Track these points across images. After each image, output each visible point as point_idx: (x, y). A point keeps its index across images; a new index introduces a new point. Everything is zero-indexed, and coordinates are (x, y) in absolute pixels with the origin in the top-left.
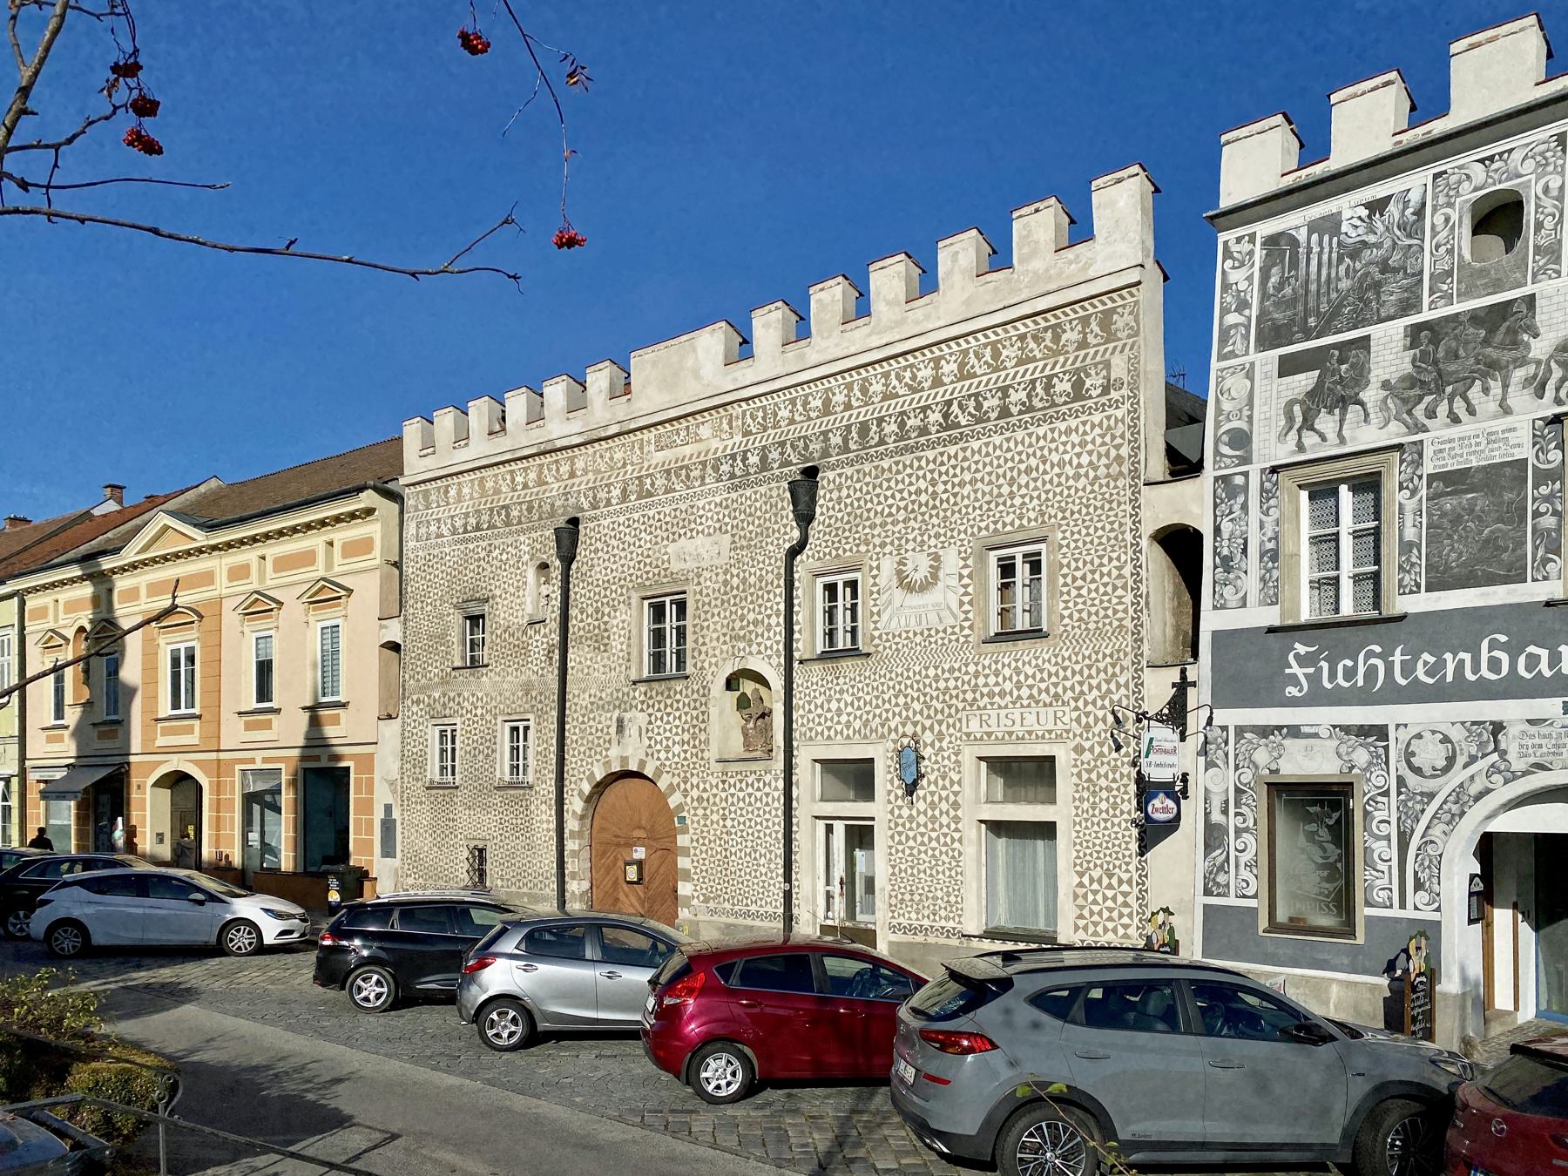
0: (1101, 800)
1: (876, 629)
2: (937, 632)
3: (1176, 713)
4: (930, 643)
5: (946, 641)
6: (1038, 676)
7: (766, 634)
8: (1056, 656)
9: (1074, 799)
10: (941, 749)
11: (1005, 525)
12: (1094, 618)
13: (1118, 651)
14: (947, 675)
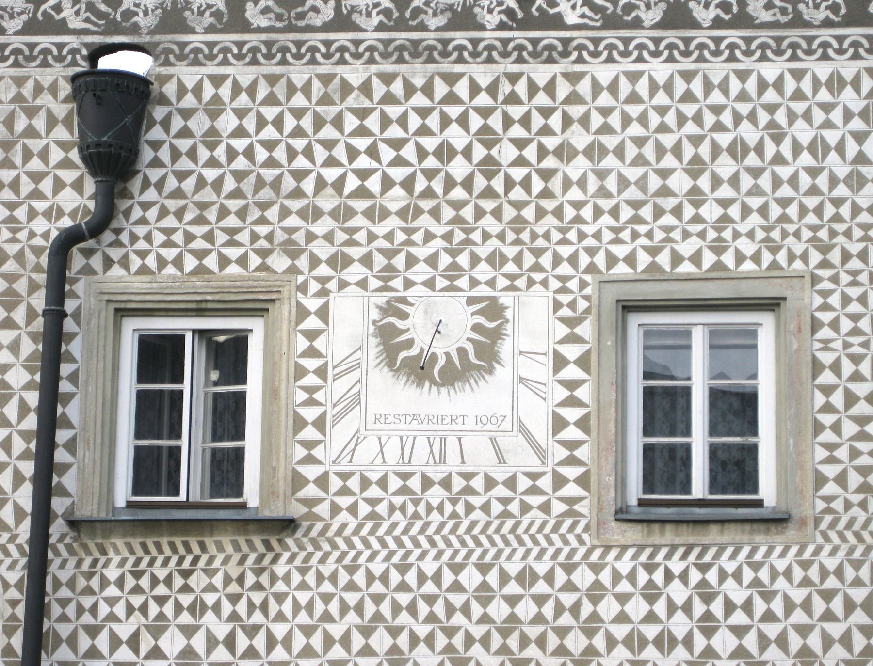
1: (310, 460)
2: (490, 483)
4: (469, 508)
5: (514, 508)
6: (759, 606)
8: (805, 565)
11: (676, 259)
14: (513, 588)
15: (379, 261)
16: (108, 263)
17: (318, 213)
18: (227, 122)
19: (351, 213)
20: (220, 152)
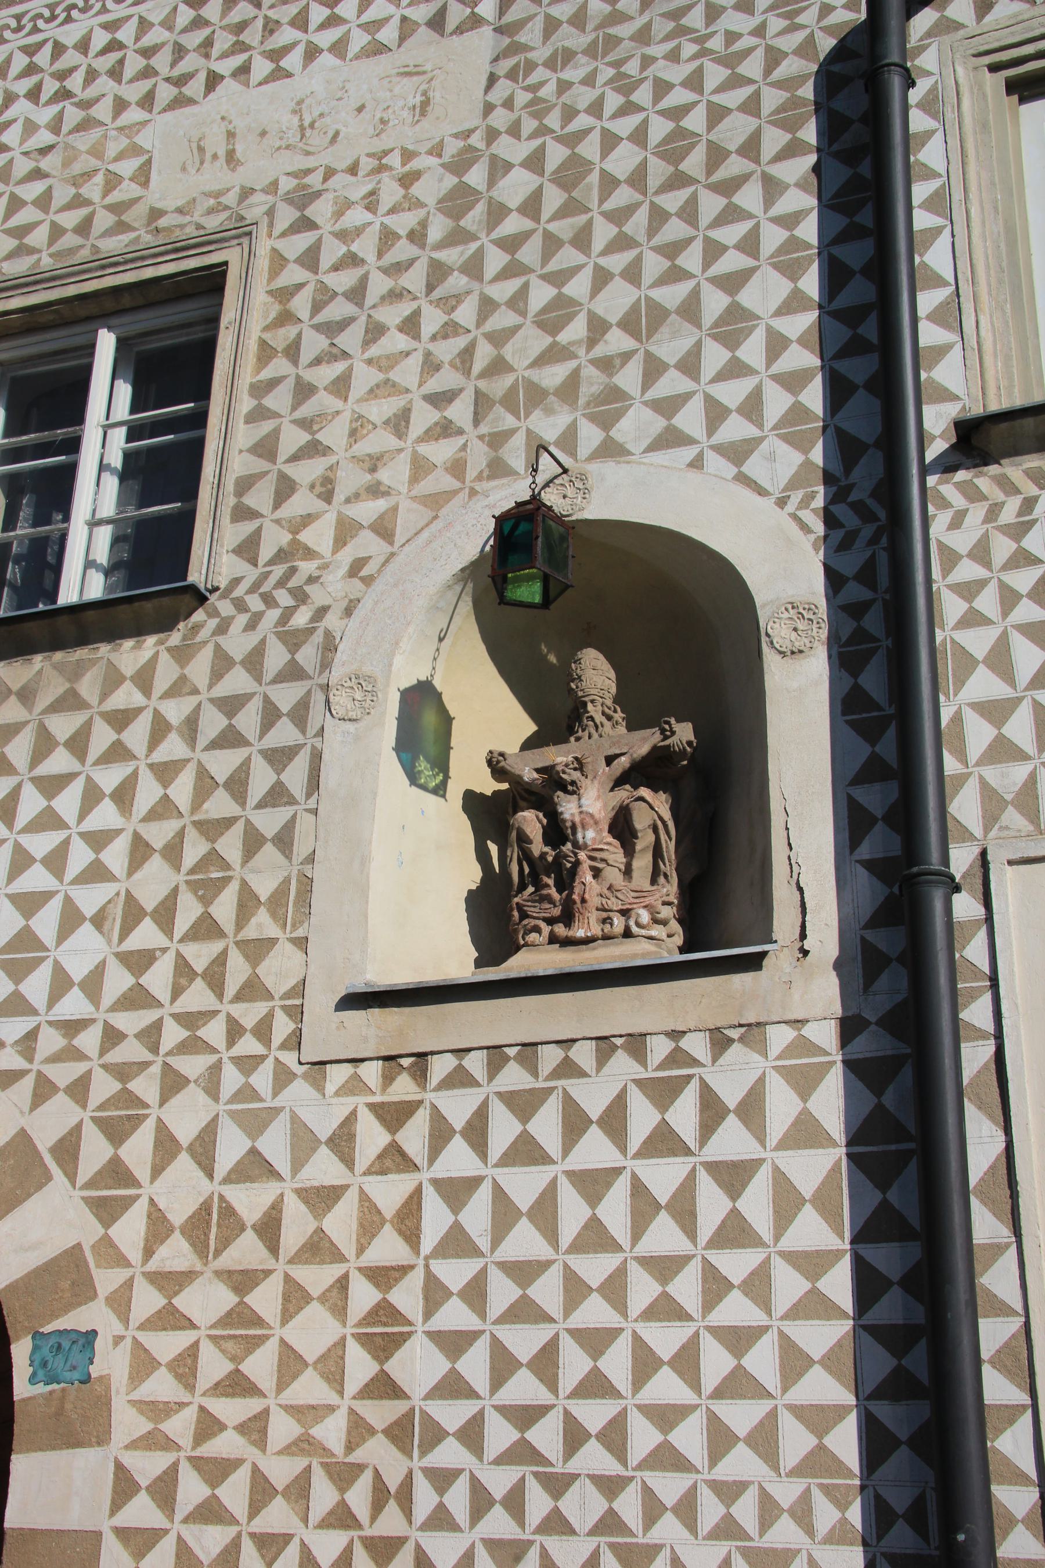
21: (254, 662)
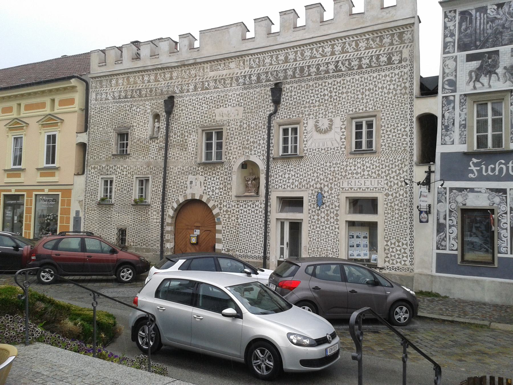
0: (396, 214)
1: (305, 147)
2: (331, 149)
3: (427, 182)
4: (328, 153)
5: (334, 153)
6: (372, 167)
7: (258, 147)
8: (379, 160)
9: (385, 213)
10: (331, 193)
11: (359, 110)
12: (394, 146)
13: (404, 159)
14: (334, 166)
15: (315, 114)
16: (277, 118)
17: (306, 107)
18: (293, 93)
19: (311, 107)
20: (292, 99)
21: (227, 168)
